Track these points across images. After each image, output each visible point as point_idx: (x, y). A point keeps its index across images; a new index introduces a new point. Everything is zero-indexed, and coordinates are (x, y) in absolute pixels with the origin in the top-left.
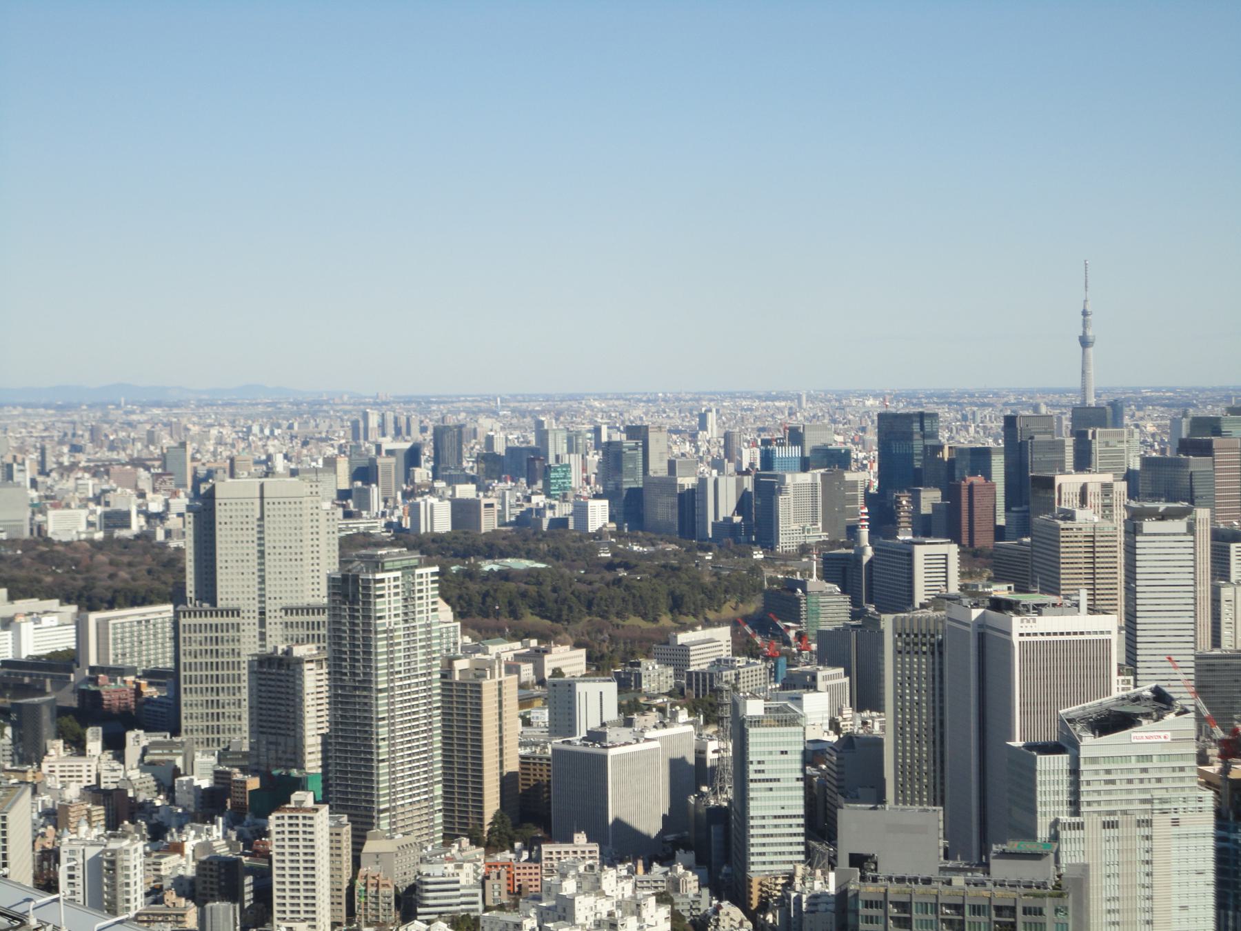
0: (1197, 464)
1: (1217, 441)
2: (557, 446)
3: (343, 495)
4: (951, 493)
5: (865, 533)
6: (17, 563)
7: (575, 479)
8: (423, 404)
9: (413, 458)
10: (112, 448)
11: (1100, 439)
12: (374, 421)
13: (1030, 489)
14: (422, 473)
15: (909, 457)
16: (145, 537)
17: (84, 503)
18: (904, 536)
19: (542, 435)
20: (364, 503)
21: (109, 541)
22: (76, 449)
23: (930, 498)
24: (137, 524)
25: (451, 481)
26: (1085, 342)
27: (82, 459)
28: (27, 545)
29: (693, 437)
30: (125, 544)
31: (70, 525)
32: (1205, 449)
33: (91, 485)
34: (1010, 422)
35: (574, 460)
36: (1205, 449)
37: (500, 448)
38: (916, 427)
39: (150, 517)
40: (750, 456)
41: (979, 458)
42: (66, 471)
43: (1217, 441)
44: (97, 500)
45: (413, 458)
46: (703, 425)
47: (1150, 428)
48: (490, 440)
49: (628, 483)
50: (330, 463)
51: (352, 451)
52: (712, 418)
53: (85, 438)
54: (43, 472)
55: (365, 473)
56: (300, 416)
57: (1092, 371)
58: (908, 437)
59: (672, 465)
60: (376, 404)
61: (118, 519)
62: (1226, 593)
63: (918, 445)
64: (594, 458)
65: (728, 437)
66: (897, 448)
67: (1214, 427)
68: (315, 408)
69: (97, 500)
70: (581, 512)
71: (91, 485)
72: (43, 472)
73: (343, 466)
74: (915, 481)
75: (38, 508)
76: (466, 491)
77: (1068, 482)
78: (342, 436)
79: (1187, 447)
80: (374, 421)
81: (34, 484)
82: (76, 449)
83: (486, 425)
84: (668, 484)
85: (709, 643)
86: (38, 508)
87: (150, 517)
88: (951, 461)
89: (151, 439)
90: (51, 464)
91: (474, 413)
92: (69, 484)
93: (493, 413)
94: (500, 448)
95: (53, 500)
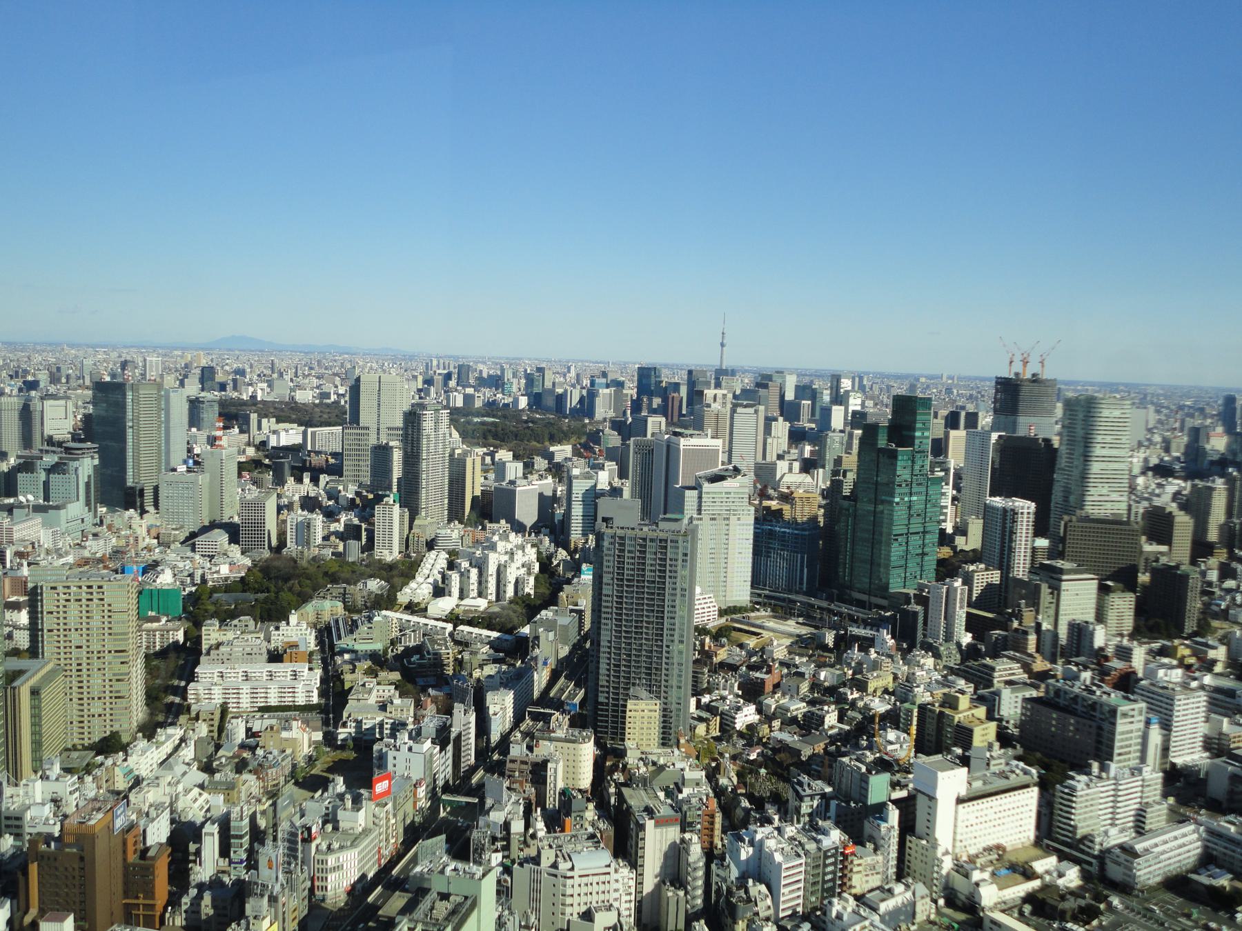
0: (762, 392)
2: (508, 375)
3: (420, 391)
4: (665, 400)
6: (282, 410)
7: (515, 389)
8: (456, 358)
9: (448, 377)
10: (326, 369)
11: (724, 380)
12: (435, 363)
13: (696, 395)
14: (452, 383)
15: (650, 385)
16: (336, 403)
17: (312, 389)
18: (644, 413)
19: (503, 370)
20: (428, 394)
21: (321, 404)
22: (311, 368)
23: (657, 402)
24: (333, 398)
25: (464, 387)
26: (722, 345)
27: (313, 372)
28: (287, 404)
29: (565, 376)
30: (328, 405)
31: (305, 396)
32: (766, 386)
33: (315, 382)
34: (690, 372)
35: (515, 381)
36: (766, 386)
37: (485, 375)
39: (339, 395)
40: (586, 382)
41: (676, 386)
42: (305, 376)
44: (318, 387)
45: (448, 377)
46: (569, 371)
48: (481, 371)
49: (536, 390)
50: (415, 377)
51: (426, 373)
52: (572, 369)
53: (315, 364)
54: (296, 376)
55: (429, 382)
56: (404, 361)
58: (649, 376)
59: (554, 384)
60: (438, 358)
61: (328, 395)
62: (769, 440)
63: (653, 380)
64: (523, 381)
65: (578, 375)
66: (644, 381)
67: (770, 378)
68: (412, 358)
69: (318, 387)
70: (516, 401)
71: (315, 382)
72: (296, 376)
73: (420, 379)
74: (651, 395)
75: (292, 390)
76: (470, 391)
77: (709, 393)
78: (421, 369)
79: (758, 385)
80: (435, 363)
81: (292, 380)
82: (311, 368)
83: (480, 367)
84: (552, 391)
85: (562, 451)
86: (292, 390)
87: (339, 395)
89: (342, 365)
90: (300, 372)
91: (476, 363)
92: (307, 381)
93: (484, 363)
94: (485, 375)
95: (299, 387)
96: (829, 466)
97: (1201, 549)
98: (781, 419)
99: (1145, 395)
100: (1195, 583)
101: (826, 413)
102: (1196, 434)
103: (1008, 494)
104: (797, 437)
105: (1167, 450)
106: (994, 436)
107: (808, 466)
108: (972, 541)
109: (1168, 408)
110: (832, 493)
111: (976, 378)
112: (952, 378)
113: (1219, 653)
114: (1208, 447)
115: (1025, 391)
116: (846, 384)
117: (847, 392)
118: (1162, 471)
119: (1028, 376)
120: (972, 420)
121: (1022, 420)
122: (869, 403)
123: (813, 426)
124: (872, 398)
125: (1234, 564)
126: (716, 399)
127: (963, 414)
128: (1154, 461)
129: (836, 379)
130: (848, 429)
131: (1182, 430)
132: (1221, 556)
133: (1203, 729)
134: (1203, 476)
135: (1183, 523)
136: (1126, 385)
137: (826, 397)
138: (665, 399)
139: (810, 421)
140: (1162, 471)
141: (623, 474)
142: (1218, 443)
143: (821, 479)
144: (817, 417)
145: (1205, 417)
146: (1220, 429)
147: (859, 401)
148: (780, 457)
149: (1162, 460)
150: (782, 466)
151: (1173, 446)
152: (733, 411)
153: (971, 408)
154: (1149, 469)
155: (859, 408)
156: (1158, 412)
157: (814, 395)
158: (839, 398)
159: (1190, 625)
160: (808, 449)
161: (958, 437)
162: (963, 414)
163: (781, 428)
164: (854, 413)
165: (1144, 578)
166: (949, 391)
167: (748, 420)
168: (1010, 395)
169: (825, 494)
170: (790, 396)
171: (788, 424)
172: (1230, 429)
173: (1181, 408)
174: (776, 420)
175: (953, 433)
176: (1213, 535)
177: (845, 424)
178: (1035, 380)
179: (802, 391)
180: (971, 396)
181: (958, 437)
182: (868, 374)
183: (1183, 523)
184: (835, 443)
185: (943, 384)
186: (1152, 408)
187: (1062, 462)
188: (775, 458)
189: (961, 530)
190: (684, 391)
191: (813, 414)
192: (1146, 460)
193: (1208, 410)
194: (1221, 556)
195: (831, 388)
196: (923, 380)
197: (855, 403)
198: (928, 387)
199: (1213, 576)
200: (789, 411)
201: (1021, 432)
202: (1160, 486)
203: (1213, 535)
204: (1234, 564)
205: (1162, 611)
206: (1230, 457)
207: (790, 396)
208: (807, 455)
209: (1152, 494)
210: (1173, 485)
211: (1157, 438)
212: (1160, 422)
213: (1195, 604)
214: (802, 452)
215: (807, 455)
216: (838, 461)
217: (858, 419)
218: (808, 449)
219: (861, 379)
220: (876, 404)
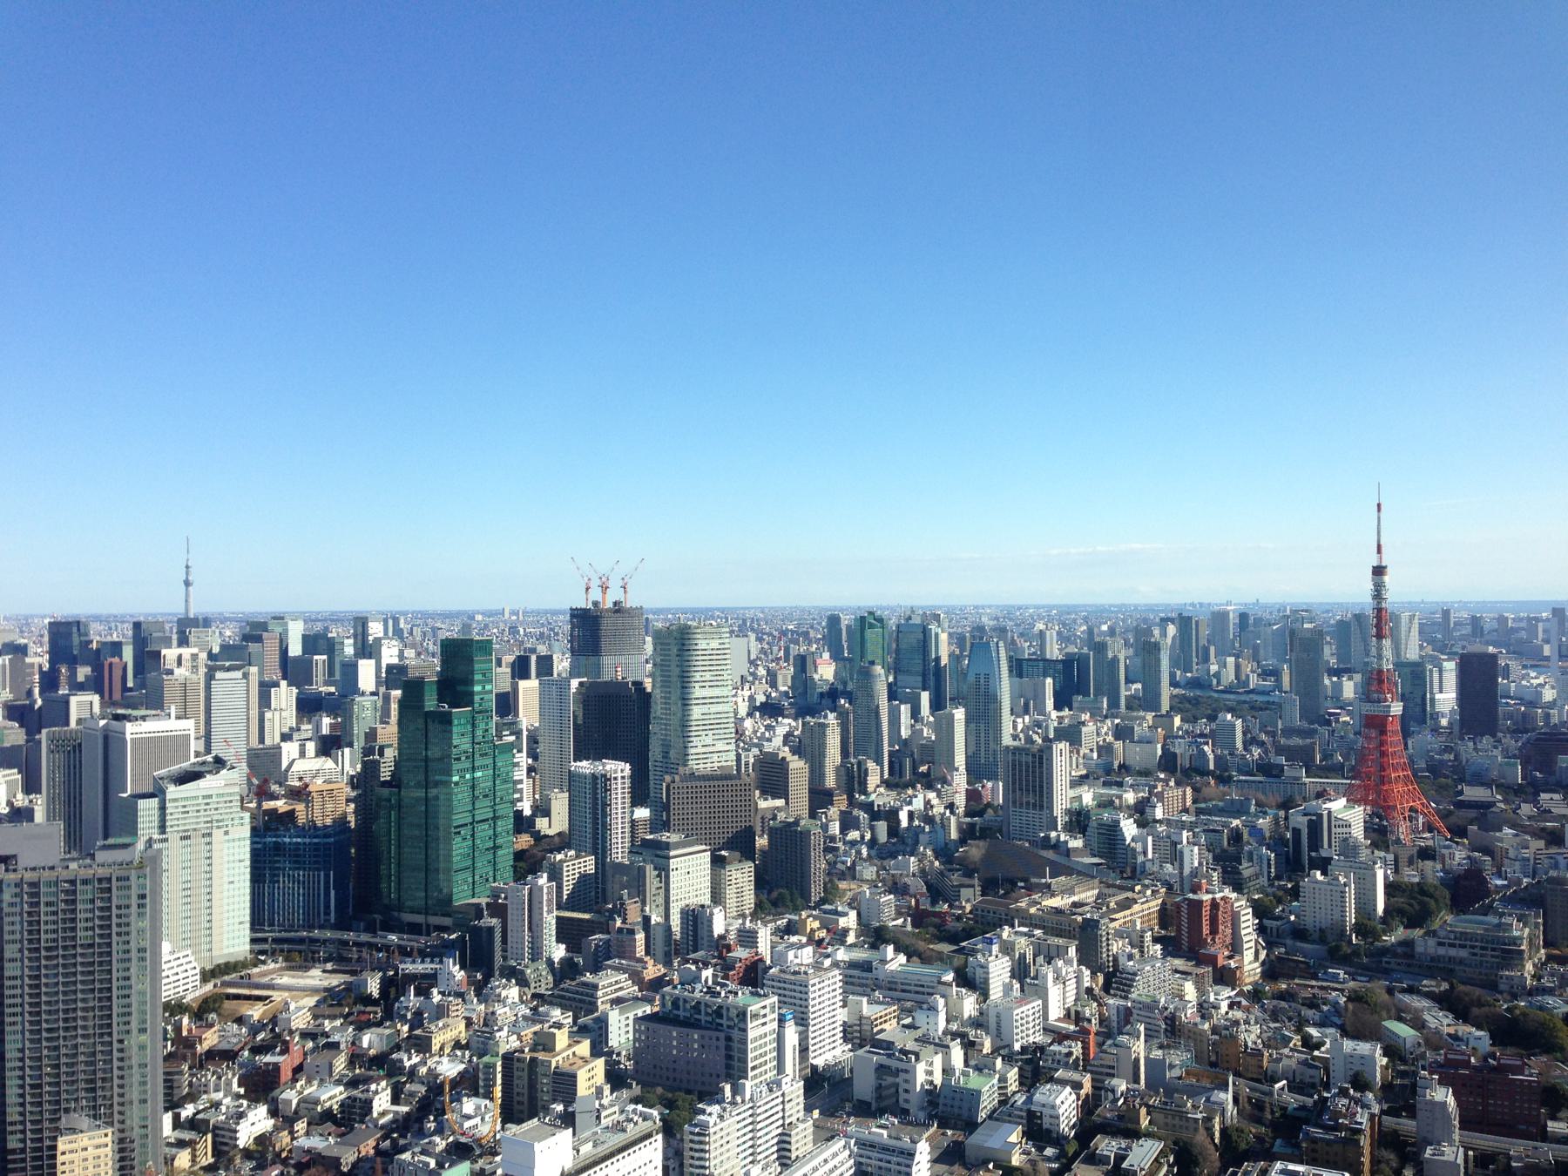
0: (253, 647)
1: (265, 635)
4: (98, 668)
5: (37, 691)
11: (193, 634)
13: (148, 658)
23: (83, 672)
26: (187, 583)
32: (259, 639)
34: (137, 626)
36: (259, 639)
38: (75, 629)
41: (116, 648)
43: (265, 635)
47: (228, 633)
57: (191, 600)
62: (268, 715)
63: (76, 640)
67: (263, 626)
74: (73, 662)
77: (170, 654)
79: (247, 638)
88: (98, 650)
96: (359, 744)
97: (820, 798)
98: (284, 683)
99: (744, 621)
100: (817, 841)
101: (351, 670)
102: (802, 664)
103: (598, 756)
104: (308, 706)
105: (773, 684)
106: (575, 683)
107: (328, 746)
108: (556, 823)
109: (770, 634)
110: (365, 781)
111: (546, 612)
112: (513, 613)
113: (850, 921)
114: (817, 677)
115: (606, 625)
116: (375, 629)
117: (378, 641)
118: (770, 710)
119: (609, 605)
120: (546, 664)
121: (607, 661)
122: (410, 653)
123: (332, 689)
124: (413, 646)
125: (855, 812)
126: (181, 663)
127: (533, 658)
128: (761, 699)
129: (361, 623)
130: (382, 690)
131: (787, 660)
132: (840, 804)
133: (842, 1015)
134: (813, 711)
135: (797, 765)
136: (722, 610)
137: (349, 650)
138: (98, 668)
139: (327, 683)
140: (770, 710)
141: (31, 786)
142: (826, 671)
143: (349, 762)
144: (337, 677)
145: (810, 644)
146: (826, 655)
147: (395, 651)
148: (286, 737)
149: (769, 697)
150: (290, 750)
151: (780, 679)
152: (210, 677)
153: (542, 650)
154: (756, 708)
155: (395, 661)
156: (759, 640)
157: (331, 647)
158: (367, 649)
159: (816, 892)
160: (326, 721)
161: (529, 688)
162: (533, 658)
163: (285, 697)
164: (390, 668)
165: (762, 842)
166: (513, 630)
167: (233, 689)
168: (589, 629)
169: (354, 782)
170: (295, 649)
171: (295, 690)
172: (836, 656)
173: (784, 633)
174: (277, 685)
175: (523, 684)
176: (830, 781)
177: (378, 684)
178: (618, 608)
179: (312, 643)
180: (542, 634)
181: (529, 688)
182: (405, 614)
183: (797, 765)
184: (365, 711)
185: (505, 622)
186: (752, 636)
187: (657, 709)
188: (277, 739)
189: (542, 809)
190: (128, 654)
191: (331, 673)
192: (752, 699)
193: (812, 634)
194: (840, 804)
195: (355, 636)
196: (479, 618)
197: (390, 655)
198: (486, 626)
199: (835, 828)
200: (295, 671)
201: (606, 678)
202: (769, 728)
203: (830, 781)
204: (855, 812)
205: (784, 880)
206: (840, 687)
207: (295, 649)
208: (325, 731)
209: (762, 738)
210: (785, 725)
211: (762, 672)
212: (762, 651)
213: (818, 864)
214: (318, 727)
215: (325, 731)
216: (371, 735)
217: (394, 676)
218: (326, 721)
219: (396, 621)
220: (419, 654)
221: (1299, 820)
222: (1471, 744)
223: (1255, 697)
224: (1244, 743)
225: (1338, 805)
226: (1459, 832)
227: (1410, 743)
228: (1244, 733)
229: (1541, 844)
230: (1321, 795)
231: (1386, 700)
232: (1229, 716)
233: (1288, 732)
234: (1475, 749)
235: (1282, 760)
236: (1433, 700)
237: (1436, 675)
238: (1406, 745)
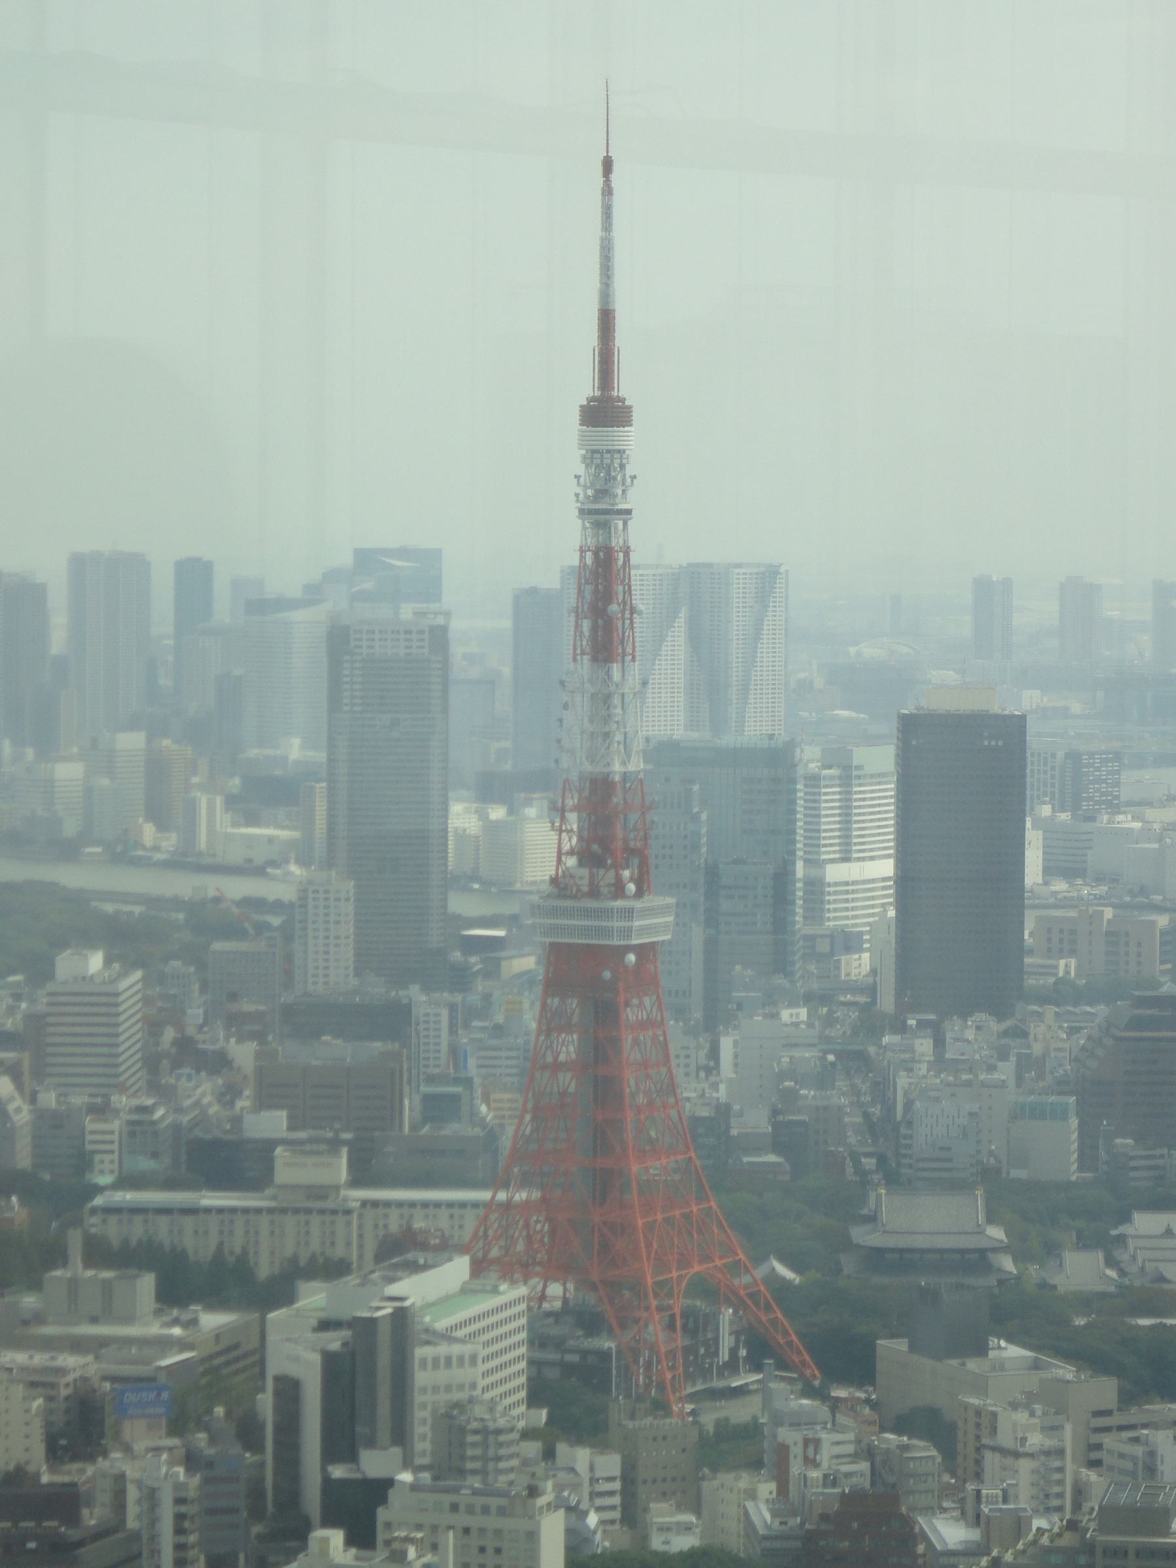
221: (295, 1345)
222: (924, 1046)
223: (212, 885)
224: (152, 1063)
225: (435, 1289)
226: (843, 1358)
227: (727, 1045)
228: (154, 1027)
229: (1104, 1390)
230: (403, 1250)
231: (619, 890)
232: (96, 962)
233: (309, 1019)
234: (939, 1062)
235: (271, 1123)
236: (816, 887)
237: (830, 796)
238: (714, 1052)
